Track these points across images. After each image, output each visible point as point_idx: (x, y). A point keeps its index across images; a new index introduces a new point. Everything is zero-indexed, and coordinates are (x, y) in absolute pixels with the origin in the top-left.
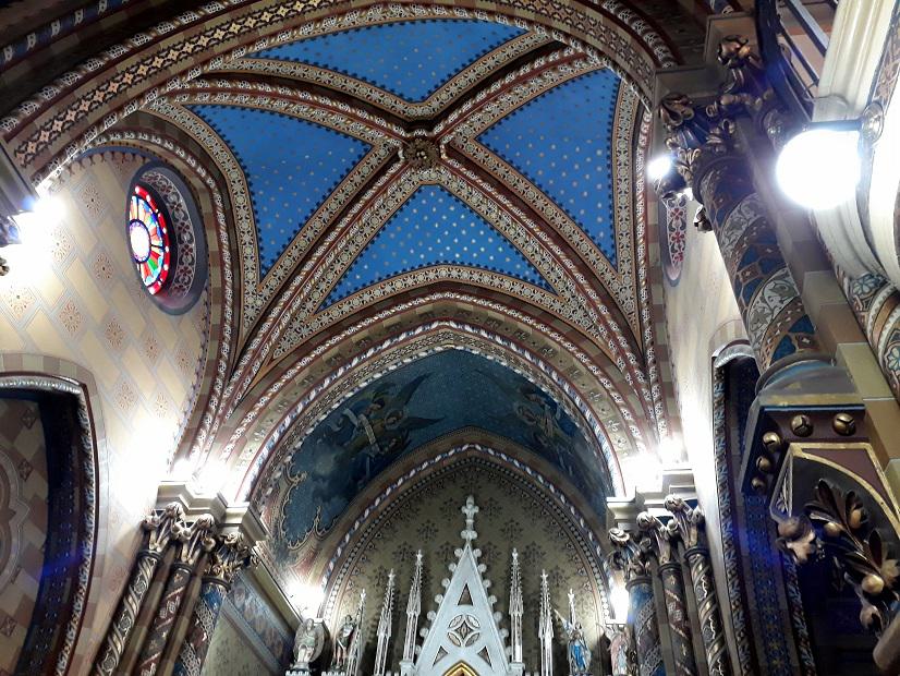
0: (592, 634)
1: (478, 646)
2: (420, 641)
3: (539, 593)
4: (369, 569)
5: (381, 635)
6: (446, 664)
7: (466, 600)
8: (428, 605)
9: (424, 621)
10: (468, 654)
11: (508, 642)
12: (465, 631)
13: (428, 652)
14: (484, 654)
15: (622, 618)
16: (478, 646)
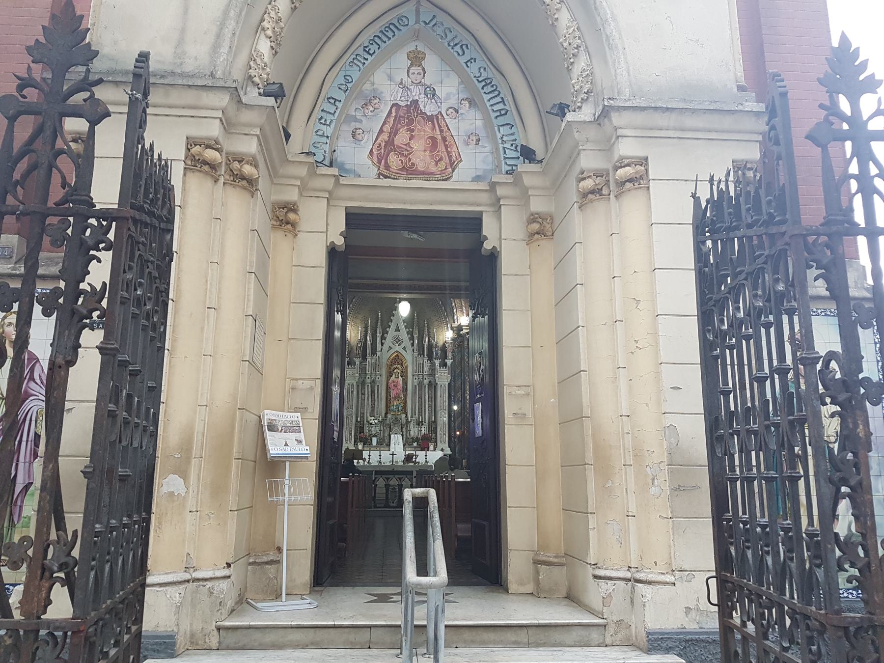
0: (441, 344)
1: (403, 346)
2: (382, 344)
3: (424, 331)
4: (360, 316)
5: (369, 342)
6: (392, 351)
7: (398, 330)
8: (385, 332)
9: (383, 338)
10: (397, 348)
11: (413, 345)
12: (397, 341)
13: (385, 347)
14: (404, 348)
15: (449, 340)
16: (403, 346)
